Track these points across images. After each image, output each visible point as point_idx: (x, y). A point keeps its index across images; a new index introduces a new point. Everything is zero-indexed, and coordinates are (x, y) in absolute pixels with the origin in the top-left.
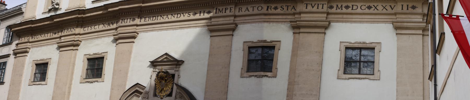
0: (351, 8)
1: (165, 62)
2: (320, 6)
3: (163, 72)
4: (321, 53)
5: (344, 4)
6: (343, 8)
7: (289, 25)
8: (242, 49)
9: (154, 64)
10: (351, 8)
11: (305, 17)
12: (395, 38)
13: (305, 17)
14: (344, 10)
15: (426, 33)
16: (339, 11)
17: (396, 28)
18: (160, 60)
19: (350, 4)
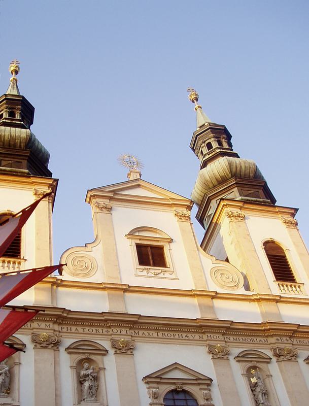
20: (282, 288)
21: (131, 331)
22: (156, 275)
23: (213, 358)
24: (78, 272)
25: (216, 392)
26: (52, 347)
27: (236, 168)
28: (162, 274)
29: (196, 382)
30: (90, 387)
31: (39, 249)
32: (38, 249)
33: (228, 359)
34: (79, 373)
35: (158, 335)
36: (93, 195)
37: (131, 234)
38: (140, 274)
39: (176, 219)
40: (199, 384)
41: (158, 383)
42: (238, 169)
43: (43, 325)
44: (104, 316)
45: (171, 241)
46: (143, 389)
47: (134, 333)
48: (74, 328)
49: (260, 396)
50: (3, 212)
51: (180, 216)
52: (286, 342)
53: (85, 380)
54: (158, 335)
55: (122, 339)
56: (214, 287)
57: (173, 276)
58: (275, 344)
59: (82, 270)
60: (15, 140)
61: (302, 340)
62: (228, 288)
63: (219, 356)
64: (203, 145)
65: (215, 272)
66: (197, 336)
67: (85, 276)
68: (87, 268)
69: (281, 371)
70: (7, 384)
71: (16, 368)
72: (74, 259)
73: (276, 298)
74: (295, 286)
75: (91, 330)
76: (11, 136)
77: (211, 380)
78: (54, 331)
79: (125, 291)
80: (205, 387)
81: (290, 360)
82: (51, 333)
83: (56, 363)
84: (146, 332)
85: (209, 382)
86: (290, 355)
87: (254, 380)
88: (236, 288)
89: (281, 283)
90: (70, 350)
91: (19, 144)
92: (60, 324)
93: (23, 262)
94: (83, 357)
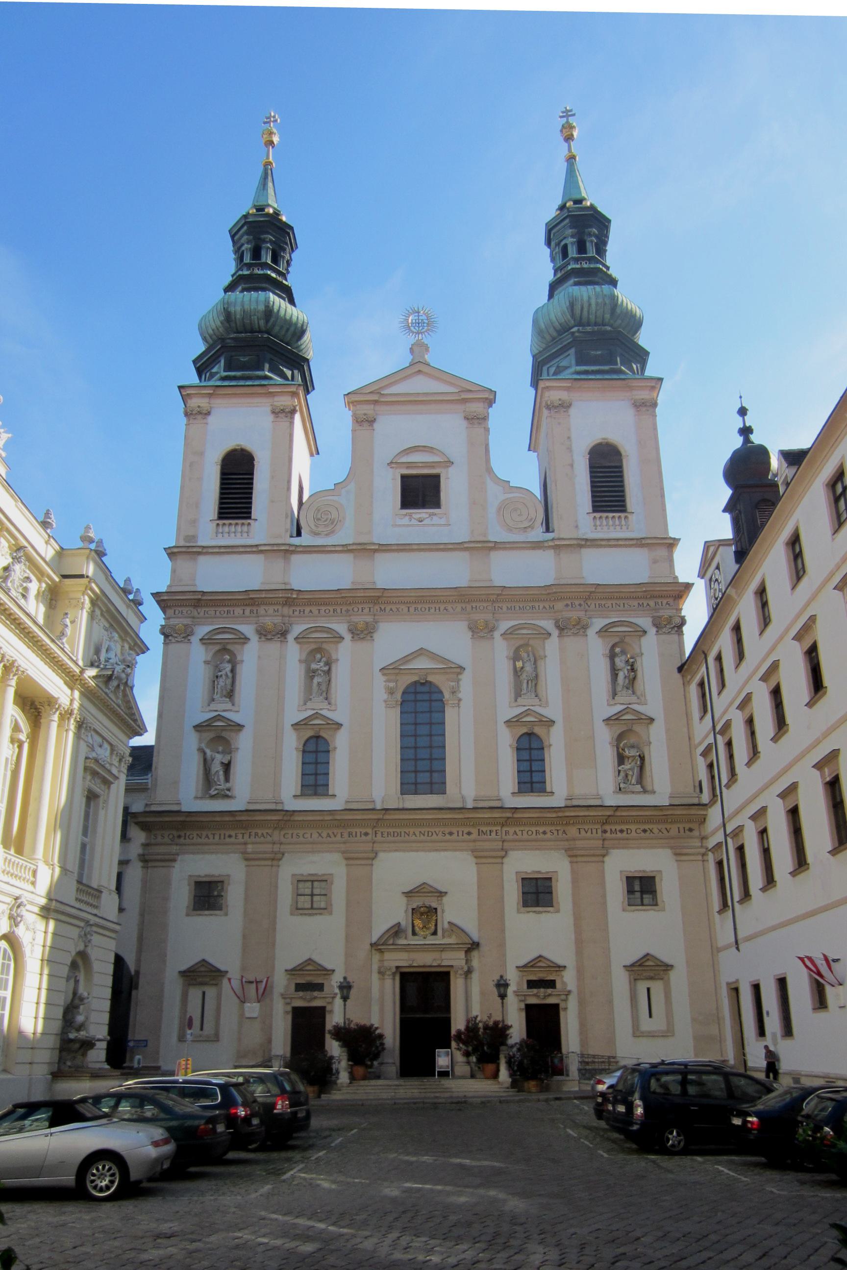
0: (625, 832)
1: (424, 892)
2: (594, 831)
3: (426, 907)
4: (602, 884)
5: (618, 828)
6: (618, 833)
8: (515, 880)
9: (409, 894)
10: (625, 832)
11: (579, 843)
12: (675, 864)
13: (579, 843)
14: (619, 835)
15: (705, 858)
16: (614, 835)
17: (676, 854)
18: (416, 890)
19: (624, 827)
20: (598, 523)
22: (421, 521)
23: (473, 637)
24: (320, 529)
28: (429, 519)
30: (319, 684)
31: (273, 502)
34: (310, 665)
36: (353, 399)
38: (399, 522)
39: (465, 424)
40: (447, 673)
42: (585, 309)
43: (271, 609)
44: (341, 594)
45: (449, 463)
46: (380, 683)
47: (379, 609)
48: (307, 609)
49: (525, 685)
51: (472, 419)
56: (497, 534)
57: (443, 521)
59: (326, 526)
60: (250, 316)
64: (557, 250)
65: (502, 508)
66: (459, 607)
70: (229, 687)
71: (238, 667)
74: (619, 517)
75: (327, 611)
76: (244, 311)
78: (283, 616)
81: (575, 634)
82: (278, 620)
87: (519, 664)
89: (598, 515)
91: (256, 322)
92: (290, 606)
94: (313, 646)
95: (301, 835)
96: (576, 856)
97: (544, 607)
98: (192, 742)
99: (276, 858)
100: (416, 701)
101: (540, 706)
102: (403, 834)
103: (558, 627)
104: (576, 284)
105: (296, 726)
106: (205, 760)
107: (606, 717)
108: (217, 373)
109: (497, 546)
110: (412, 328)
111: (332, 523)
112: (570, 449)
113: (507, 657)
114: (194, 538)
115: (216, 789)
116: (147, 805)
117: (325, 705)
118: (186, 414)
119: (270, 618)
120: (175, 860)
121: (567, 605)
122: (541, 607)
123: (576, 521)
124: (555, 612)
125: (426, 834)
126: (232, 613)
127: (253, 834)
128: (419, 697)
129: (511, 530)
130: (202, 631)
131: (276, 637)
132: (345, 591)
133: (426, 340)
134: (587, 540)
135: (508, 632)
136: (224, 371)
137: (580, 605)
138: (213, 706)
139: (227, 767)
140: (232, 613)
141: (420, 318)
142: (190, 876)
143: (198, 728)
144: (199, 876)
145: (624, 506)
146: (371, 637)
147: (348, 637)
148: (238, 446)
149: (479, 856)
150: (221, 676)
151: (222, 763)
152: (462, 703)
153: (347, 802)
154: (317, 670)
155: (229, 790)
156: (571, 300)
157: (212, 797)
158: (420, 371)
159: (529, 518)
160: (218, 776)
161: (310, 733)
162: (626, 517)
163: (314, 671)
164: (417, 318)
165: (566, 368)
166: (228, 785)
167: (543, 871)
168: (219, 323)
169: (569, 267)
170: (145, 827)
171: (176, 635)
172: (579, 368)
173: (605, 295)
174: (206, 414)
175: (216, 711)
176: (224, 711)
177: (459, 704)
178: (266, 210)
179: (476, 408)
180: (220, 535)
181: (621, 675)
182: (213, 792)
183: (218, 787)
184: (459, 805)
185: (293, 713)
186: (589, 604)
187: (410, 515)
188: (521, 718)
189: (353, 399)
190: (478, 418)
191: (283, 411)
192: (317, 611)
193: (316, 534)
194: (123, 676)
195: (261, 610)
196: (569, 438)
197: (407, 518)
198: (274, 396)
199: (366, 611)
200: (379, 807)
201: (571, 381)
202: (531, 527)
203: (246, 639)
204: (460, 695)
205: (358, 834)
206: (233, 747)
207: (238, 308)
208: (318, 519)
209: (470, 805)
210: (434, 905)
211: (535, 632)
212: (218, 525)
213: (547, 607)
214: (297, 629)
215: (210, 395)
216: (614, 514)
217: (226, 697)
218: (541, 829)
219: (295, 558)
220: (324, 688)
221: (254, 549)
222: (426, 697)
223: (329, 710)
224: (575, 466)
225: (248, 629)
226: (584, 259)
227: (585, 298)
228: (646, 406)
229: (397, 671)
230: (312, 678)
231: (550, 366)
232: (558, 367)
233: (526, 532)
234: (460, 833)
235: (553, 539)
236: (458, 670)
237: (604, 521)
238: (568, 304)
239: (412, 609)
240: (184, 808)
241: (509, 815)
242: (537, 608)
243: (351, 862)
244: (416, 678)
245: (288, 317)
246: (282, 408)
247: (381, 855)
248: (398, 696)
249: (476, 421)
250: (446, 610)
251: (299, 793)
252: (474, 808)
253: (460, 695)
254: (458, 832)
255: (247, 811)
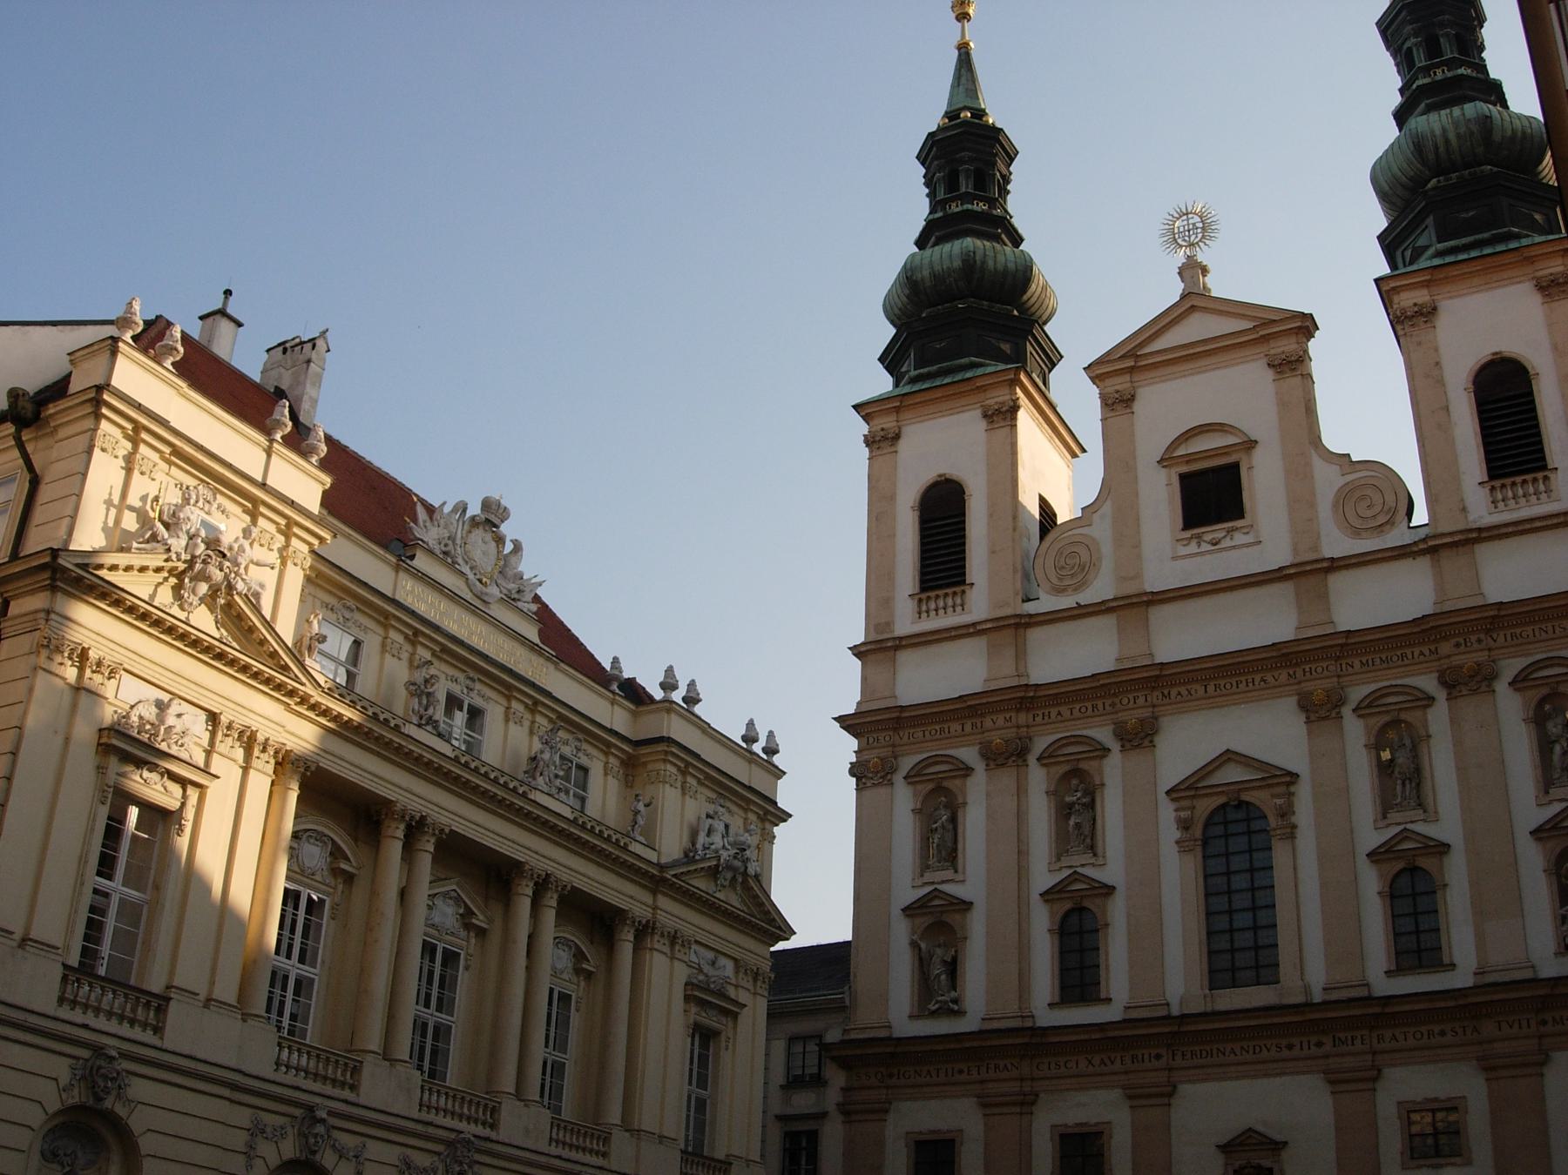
2: (1524, 1023)
3: (1252, 1167)
7: (1475, 1062)
9: (1226, 1148)
20: (1499, 496)
21: (1156, 693)
23: (1308, 721)
25: (1304, 795)
26: (1014, 761)
27: (1436, 148)
28: (1228, 538)
29: (1264, 783)
30: (1078, 826)
31: (993, 552)
32: (993, 552)
33: (1340, 717)
35: (1206, 691)
36: (1098, 371)
37: (1165, 461)
39: (1270, 374)
40: (1270, 786)
41: (1193, 797)
42: (1442, 149)
43: (1000, 721)
44: (1099, 680)
45: (1250, 445)
46: (1167, 813)
48: (1054, 712)
49: (1399, 788)
50: (931, 481)
51: (1280, 364)
52: (1476, 646)
53: (1069, 815)
54: (1206, 691)
55: (1131, 717)
56: (1337, 544)
57: (1249, 539)
58: (1449, 656)
61: (1518, 631)
62: (1364, 534)
63: (1323, 713)
66: (1283, 677)
67: (1080, 586)
68: (1082, 567)
69: (1452, 721)
71: (960, 814)
72: (1060, 552)
73: (1471, 536)
75: (1083, 710)
77: (1293, 777)
79: (1149, 603)
80: (1282, 789)
81: (1475, 692)
82: (1010, 733)
83: (1021, 791)
84: (1183, 690)
85: (1288, 779)
86: (1479, 678)
87: (1386, 755)
88: (1388, 526)
89: (1497, 483)
90: (1045, 759)
92: (1028, 710)
93: (967, 591)
95: (1062, 1064)
96: (1494, 1068)
97: (1422, 653)
98: (901, 933)
99: (1026, 1103)
100: (1226, 836)
101: (1424, 821)
102: (1215, 1052)
103: (1443, 683)
104: (1428, 110)
105: (1048, 896)
106: (921, 959)
107: (1534, 826)
108: (908, 371)
109: (1336, 565)
110: (1179, 241)
111: (1083, 569)
112: (1441, 382)
113: (1366, 746)
114: (889, 625)
115: (937, 1002)
116: (845, 1030)
117: (1087, 858)
118: (870, 441)
119: (999, 730)
120: (886, 1111)
121: (1458, 645)
122: (1416, 654)
123: (1462, 500)
124: (1439, 659)
125: (1251, 1052)
126: (946, 731)
127: (992, 1066)
128: (1233, 828)
129: (1359, 534)
130: (907, 763)
131: (1010, 761)
132: (1102, 676)
133: (1202, 256)
134: (1479, 530)
135: (1363, 705)
136: (915, 370)
137: (1479, 641)
138: (928, 877)
139: (953, 968)
140: (946, 731)
141: (1191, 221)
142: (907, 1133)
143: (909, 911)
144: (921, 1133)
145: (1544, 459)
146: (1151, 741)
147: (1115, 747)
148: (940, 476)
149: (1336, 1081)
150: (936, 829)
151: (945, 962)
152: (1299, 833)
153: (1127, 1008)
154: (1074, 803)
155: (955, 1001)
156: (1416, 140)
157: (933, 1014)
158: (1193, 306)
159: (1386, 508)
160: (939, 981)
161: (1068, 905)
162: (1546, 478)
163: (1071, 806)
164: (1186, 222)
165: (1426, 248)
166: (953, 994)
167: (1443, 1097)
168: (905, 299)
169: (1414, 86)
170: (845, 1064)
171: (871, 775)
172: (1440, 246)
173: (1469, 120)
174: (893, 438)
175: (933, 883)
176: (943, 882)
177: (1292, 833)
178: (962, 115)
179: (1287, 346)
180: (924, 615)
181: (1557, 748)
182: (933, 1007)
183: (940, 998)
184: (1300, 999)
185: (1043, 877)
186: (1495, 636)
187: (1199, 537)
188: (1396, 845)
189: (1098, 371)
190: (1289, 362)
191: (998, 412)
192: (1069, 712)
193: (1059, 591)
194: (737, 863)
195: (988, 723)
196: (1437, 363)
197: (1194, 543)
198: (985, 390)
199: (1141, 701)
200: (1175, 1011)
201: (1430, 271)
202: (1390, 523)
203: (967, 771)
204: (1294, 819)
205: (1146, 1057)
206: (959, 936)
207: (926, 273)
208: (1063, 567)
209: (1317, 998)
210: (1266, 1163)
211: (1409, 698)
212: (920, 601)
213: (1427, 653)
214: (1041, 744)
215: (897, 410)
216: (1523, 477)
217: (946, 860)
218: (1437, 1029)
219: (1035, 635)
220: (1087, 830)
221: (971, 630)
222: (1242, 827)
223: (1093, 865)
224: (1451, 408)
225: (968, 754)
226: (1438, 66)
227: (1438, 132)
228: (1558, 284)
229: (1192, 793)
230: (1068, 816)
231: (1405, 249)
232: (1414, 249)
233: (1382, 531)
234: (1305, 1045)
235: (1424, 540)
236: (1288, 779)
237: (1520, 489)
238: (1411, 145)
239: (1211, 688)
240: (897, 1034)
241: (1377, 1010)
242: (1410, 657)
243: (1136, 1103)
244: (1222, 800)
245: (1000, 267)
246: (996, 407)
247: (1185, 1089)
248: (1198, 832)
249: (1285, 368)
250: (1264, 681)
251: (1057, 999)
252: (1324, 1003)
253: (1294, 819)
254: (1301, 1043)
255: (981, 1032)
